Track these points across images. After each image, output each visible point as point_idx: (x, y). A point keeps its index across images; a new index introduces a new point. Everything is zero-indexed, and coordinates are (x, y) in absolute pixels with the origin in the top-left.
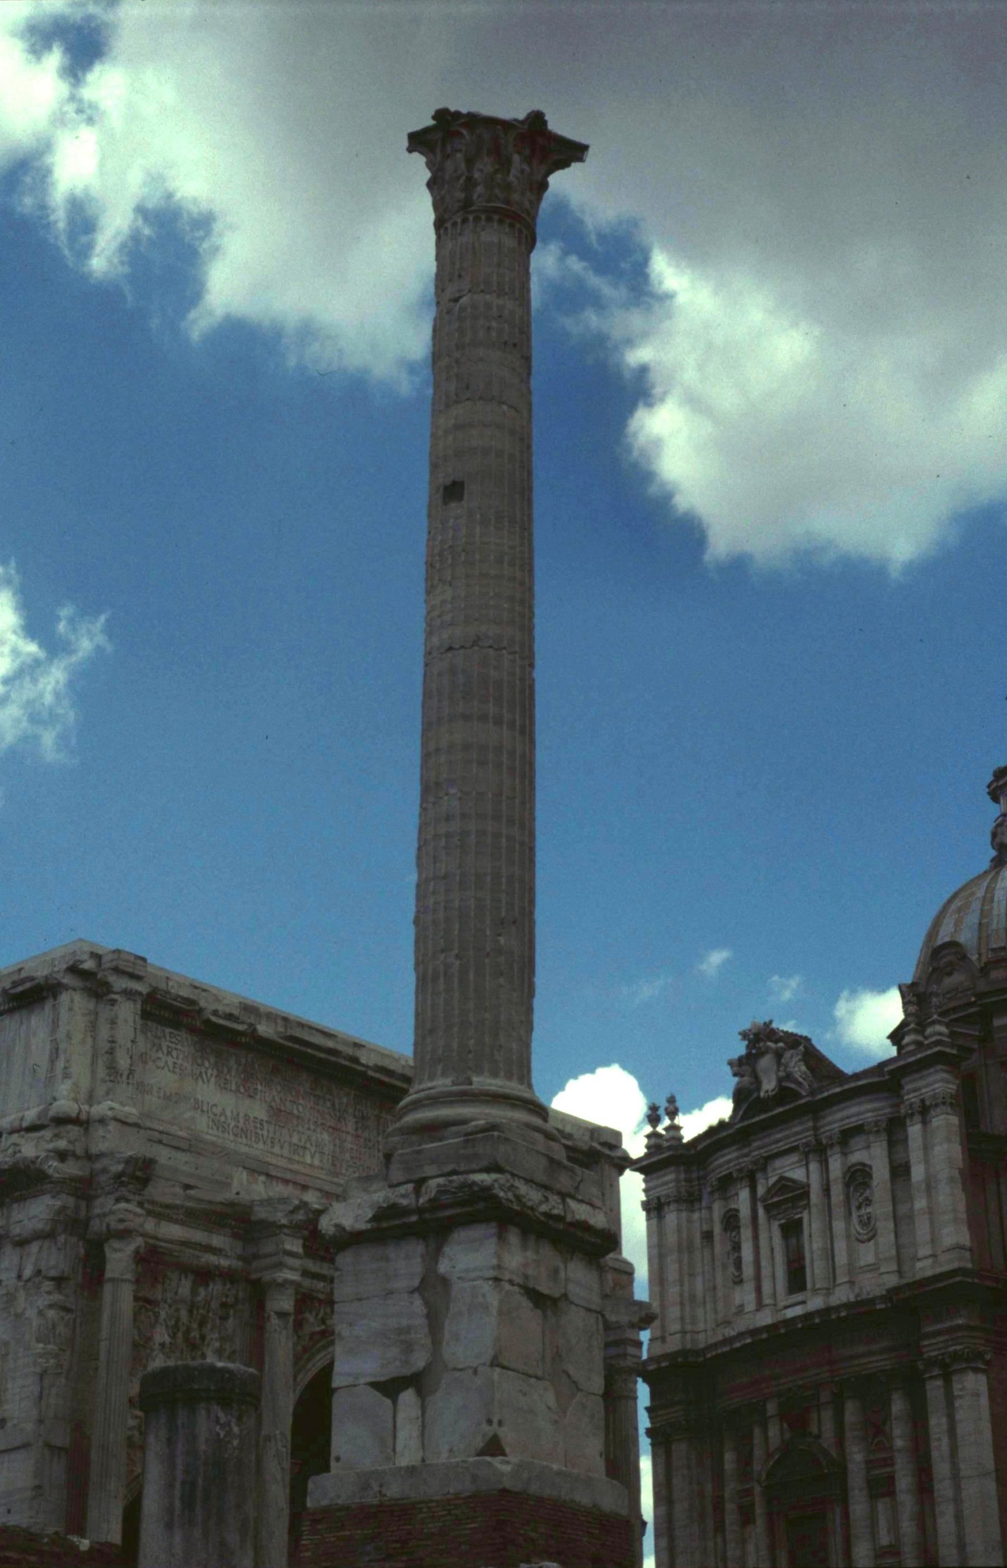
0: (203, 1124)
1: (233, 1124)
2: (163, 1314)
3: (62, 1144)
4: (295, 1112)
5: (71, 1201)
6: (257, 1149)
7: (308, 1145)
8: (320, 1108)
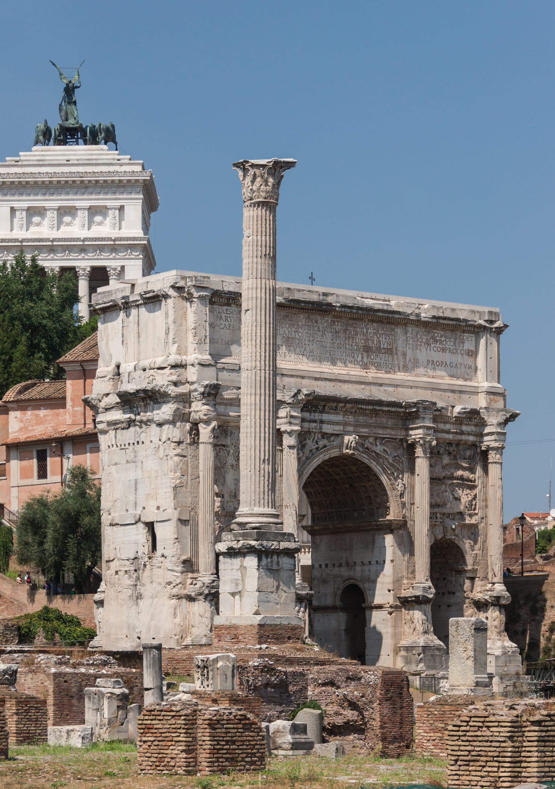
7: (305, 353)
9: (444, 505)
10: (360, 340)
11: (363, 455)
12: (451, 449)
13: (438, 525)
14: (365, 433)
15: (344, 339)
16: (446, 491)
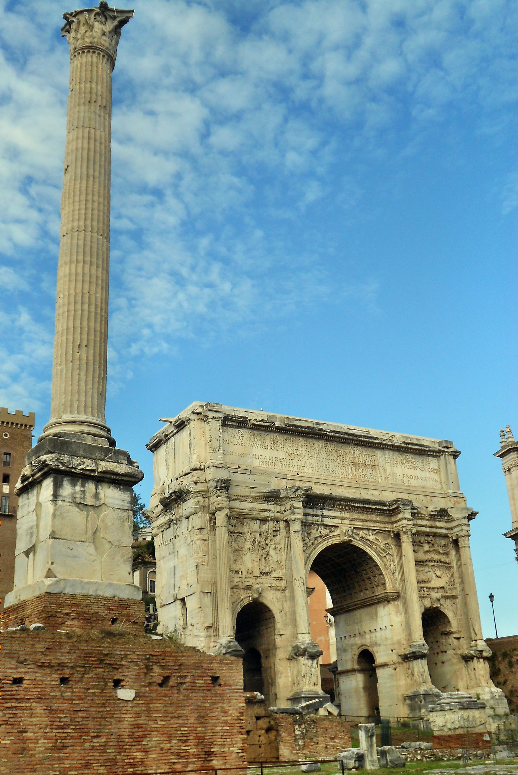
0: (256, 463)
1: (270, 461)
2: (248, 537)
3: (195, 479)
4: (298, 453)
5: (201, 500)
6: (283, 470)
7: (305, 465)
8: (309, 450)
9: (429, 581)
10: (349, 457)
11: (359, 542)
12: (429, 539)
13: (426, 597)
14: (359, 525)
15: (336, 456)
16: (430, 572)
